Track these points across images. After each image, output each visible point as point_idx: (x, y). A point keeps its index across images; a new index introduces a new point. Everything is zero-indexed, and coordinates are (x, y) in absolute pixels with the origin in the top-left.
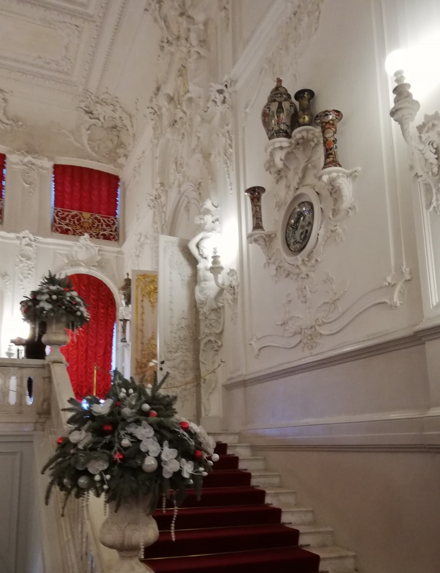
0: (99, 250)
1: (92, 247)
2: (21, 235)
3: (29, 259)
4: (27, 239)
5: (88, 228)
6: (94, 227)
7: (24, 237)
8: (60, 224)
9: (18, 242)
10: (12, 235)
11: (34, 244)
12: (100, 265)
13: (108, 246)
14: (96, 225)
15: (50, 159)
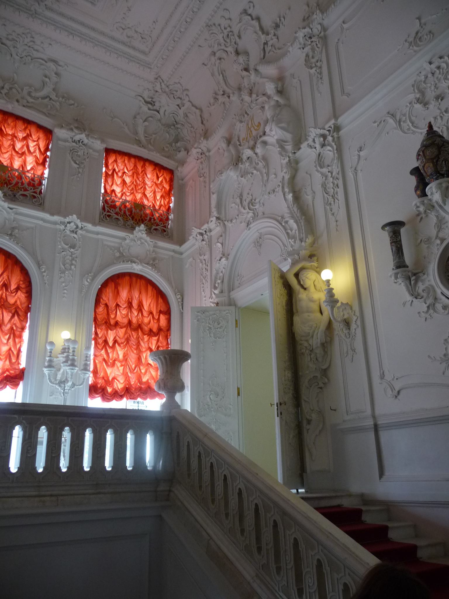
0: (155, 247)
1: (146, 241)
2: (67, 220)
3: (73, 247)
4: (72, 224)
5: (139, 220)
6: (146, 220)
7: (69, 223)
8: (108, 212)
9: (62, 227)
10: (56, 218)
11: (80, 232)
12: (153, 262)
13: (164, 241)
14: (148, 218)
15: (103, 141)
